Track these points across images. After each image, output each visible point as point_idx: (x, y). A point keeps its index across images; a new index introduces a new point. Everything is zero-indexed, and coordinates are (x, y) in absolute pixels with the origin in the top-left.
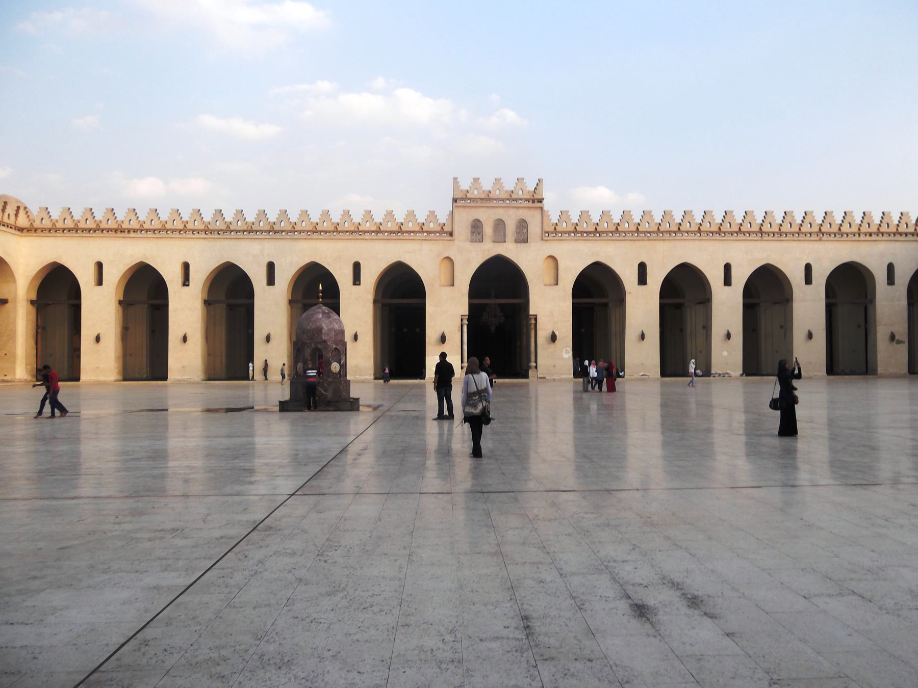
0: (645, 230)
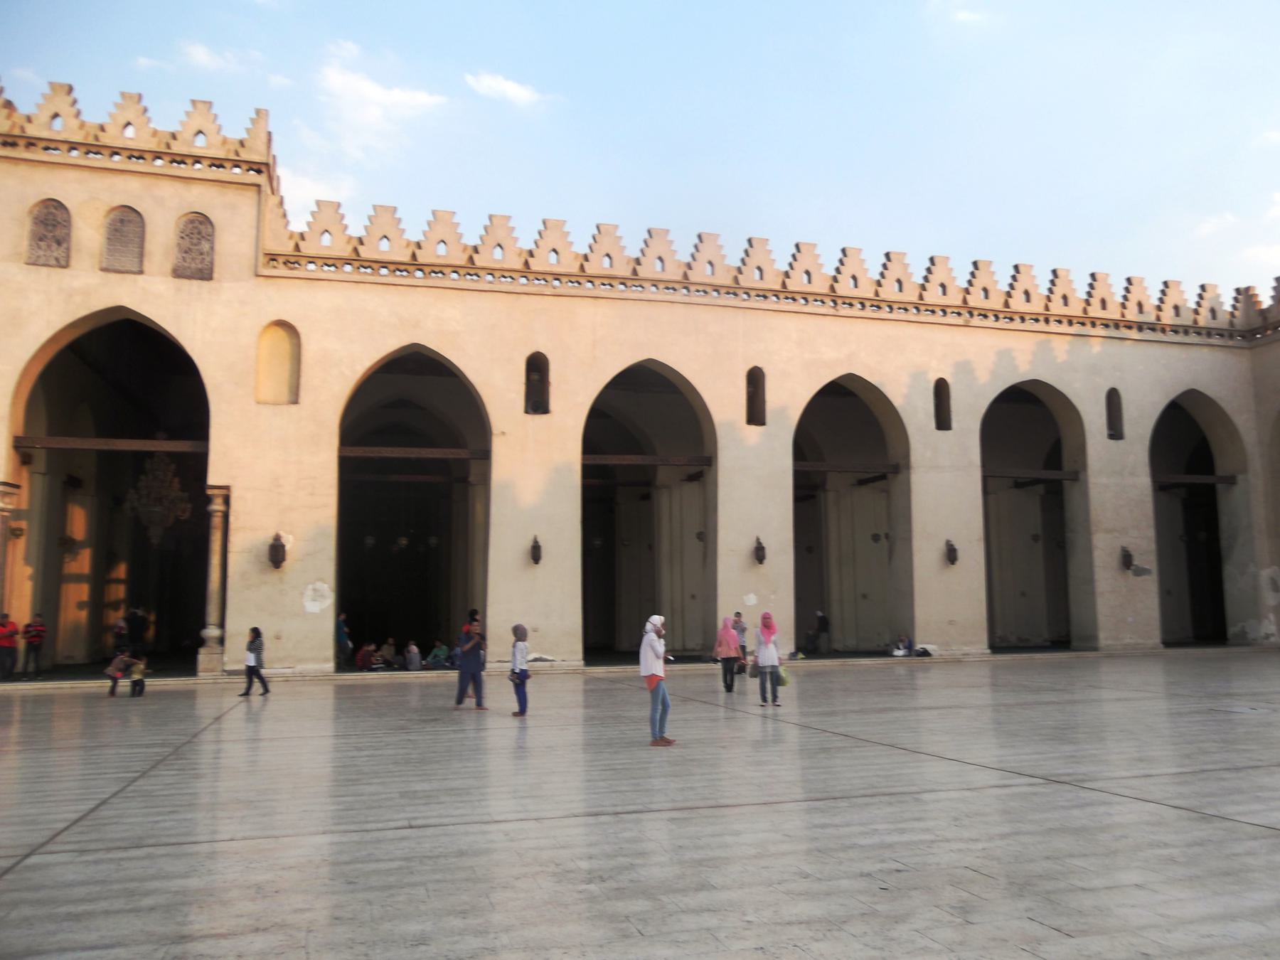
0: (548, 269)
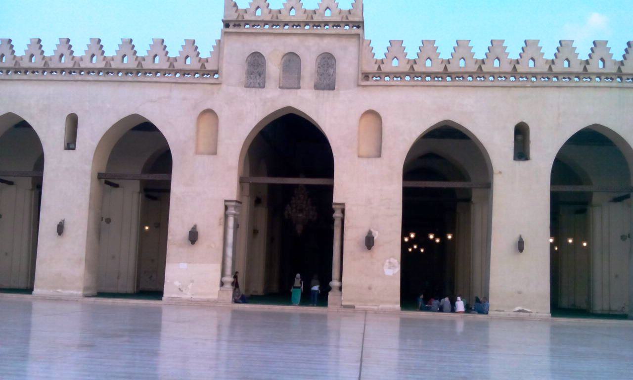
0: (528, 70)
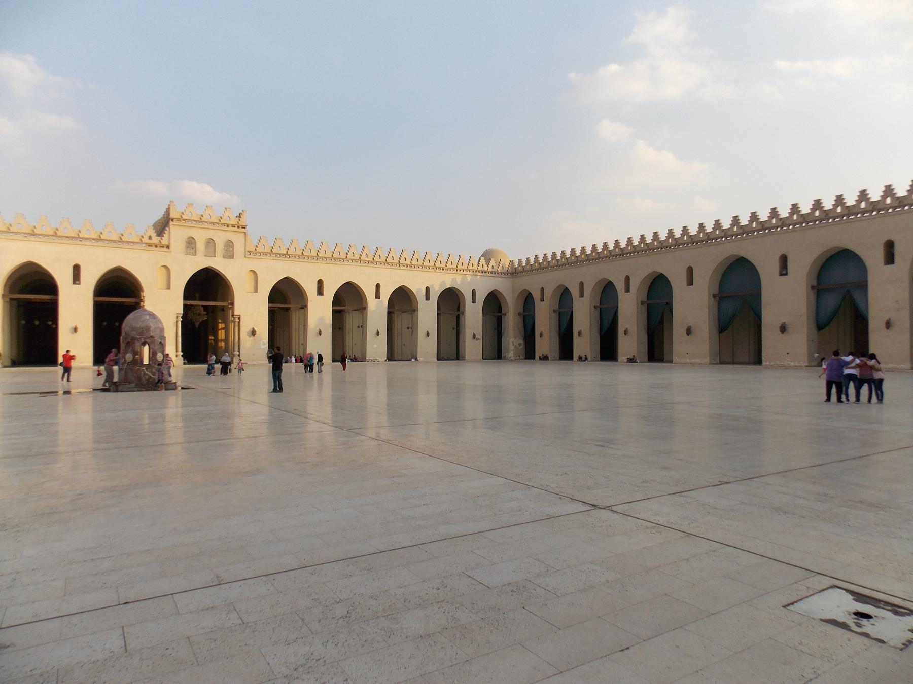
0: (323, 256)
